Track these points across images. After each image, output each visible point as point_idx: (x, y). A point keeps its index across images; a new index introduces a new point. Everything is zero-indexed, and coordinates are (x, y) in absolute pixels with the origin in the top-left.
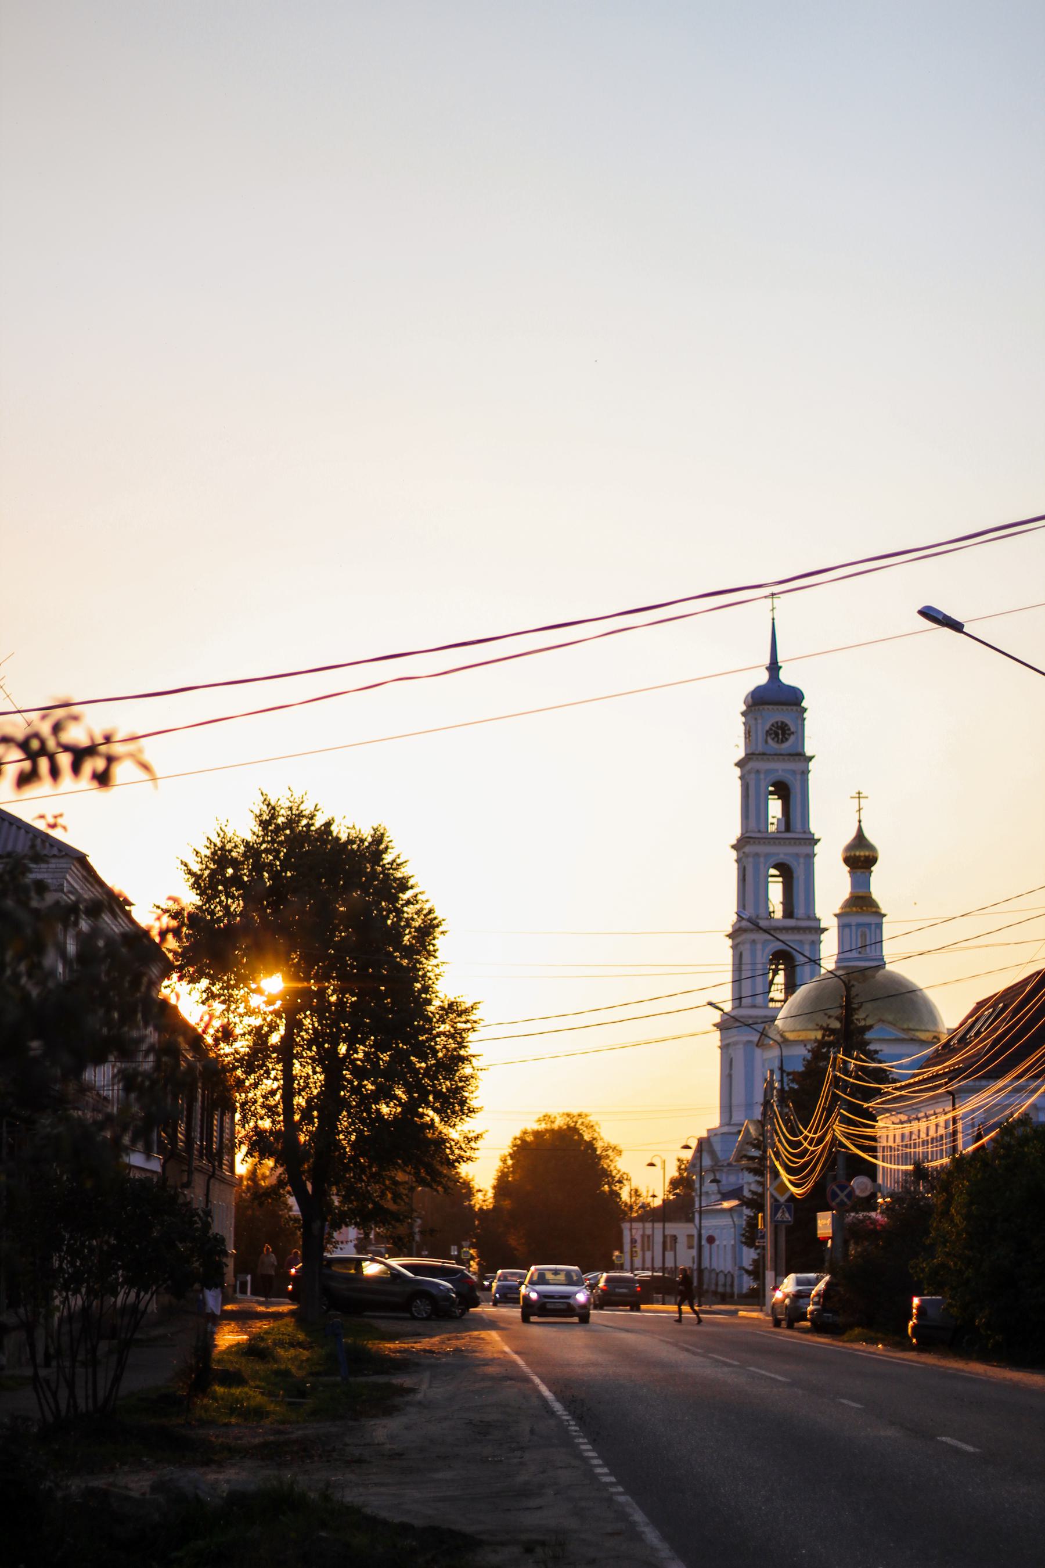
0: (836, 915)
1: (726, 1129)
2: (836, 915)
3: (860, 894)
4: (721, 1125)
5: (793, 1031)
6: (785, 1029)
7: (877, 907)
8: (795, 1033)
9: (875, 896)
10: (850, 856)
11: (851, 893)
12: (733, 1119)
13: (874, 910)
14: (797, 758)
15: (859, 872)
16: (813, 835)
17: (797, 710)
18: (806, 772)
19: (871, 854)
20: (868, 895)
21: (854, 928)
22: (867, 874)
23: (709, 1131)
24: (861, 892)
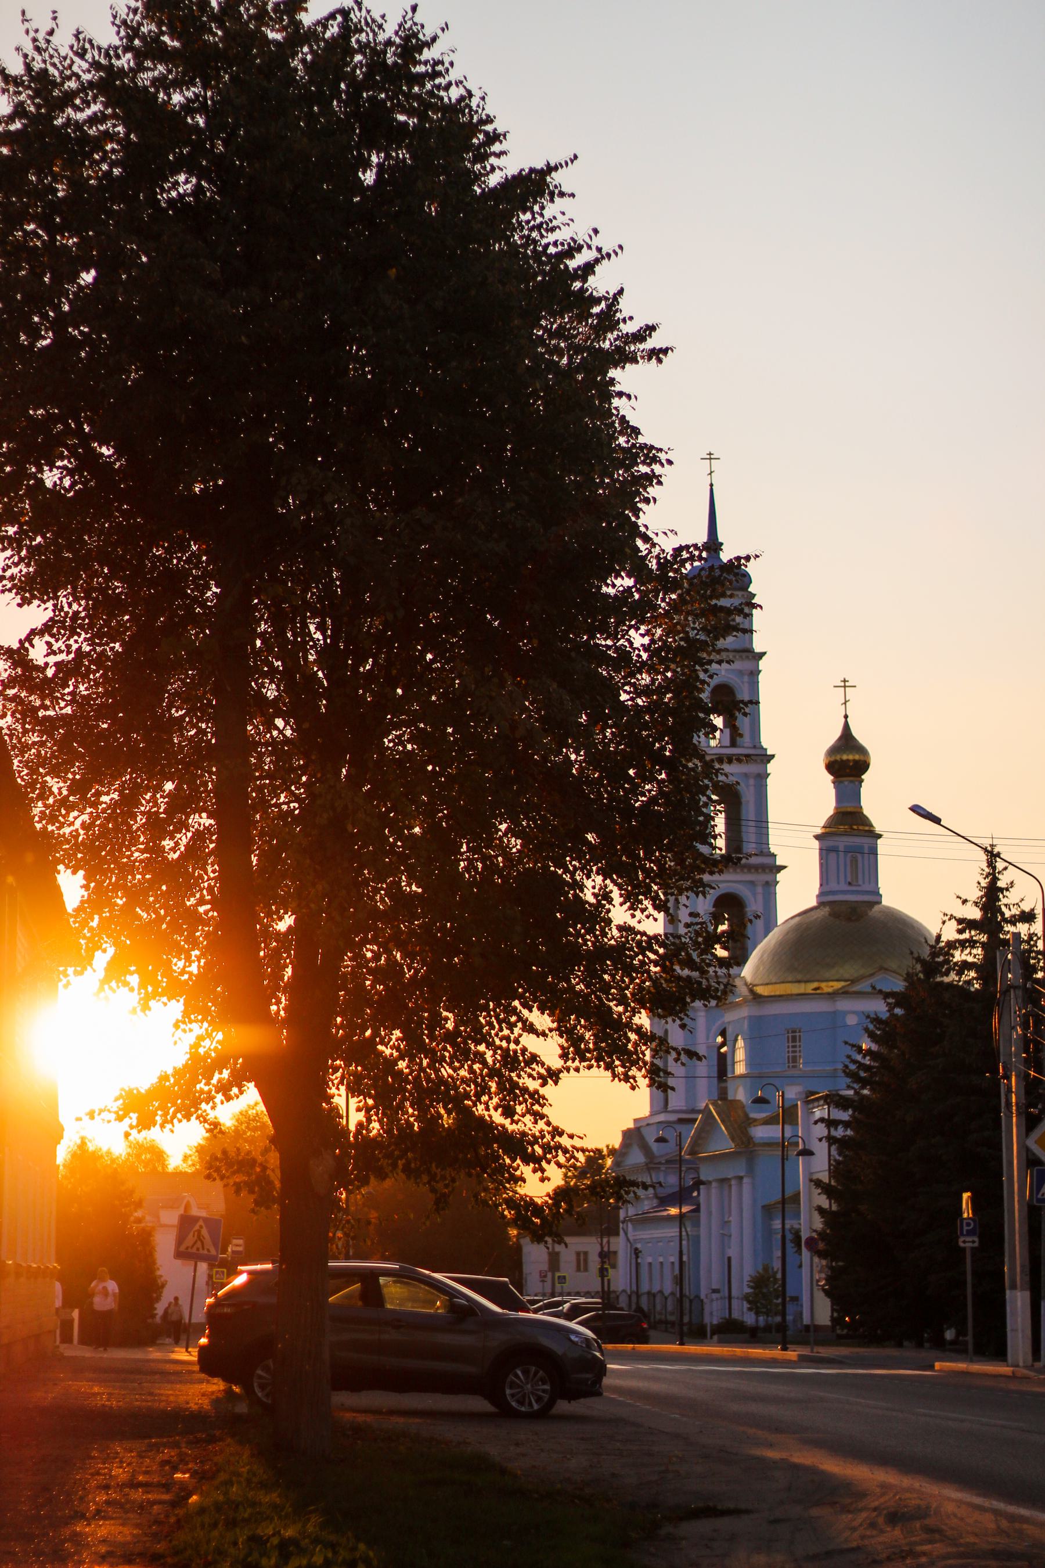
0: (817, 837)
1: (662, 1117)
2: (817, 837)
3: (849, 810)
4: (653, 1113)
5: (767, 984)
6: (756, 982)
7: (871, 825)
8: (770, 987)
9: (866, 812)
10: (836, 761)
11: (836, 808)
12: (670, 1105)
13: (867, 828)
14: (744, 655)
15: (846, 781)
16: (766, 749)
17: (743, 595)
18: (755, 673)
19: (862, 758)
20: (859, 810)
21: (841, 854)
22: (857, 783)
23: (636, 1121)
24: (849, 807)
